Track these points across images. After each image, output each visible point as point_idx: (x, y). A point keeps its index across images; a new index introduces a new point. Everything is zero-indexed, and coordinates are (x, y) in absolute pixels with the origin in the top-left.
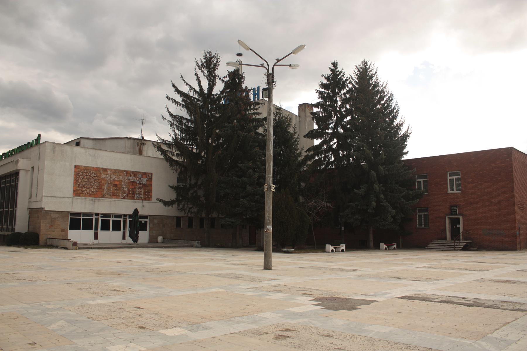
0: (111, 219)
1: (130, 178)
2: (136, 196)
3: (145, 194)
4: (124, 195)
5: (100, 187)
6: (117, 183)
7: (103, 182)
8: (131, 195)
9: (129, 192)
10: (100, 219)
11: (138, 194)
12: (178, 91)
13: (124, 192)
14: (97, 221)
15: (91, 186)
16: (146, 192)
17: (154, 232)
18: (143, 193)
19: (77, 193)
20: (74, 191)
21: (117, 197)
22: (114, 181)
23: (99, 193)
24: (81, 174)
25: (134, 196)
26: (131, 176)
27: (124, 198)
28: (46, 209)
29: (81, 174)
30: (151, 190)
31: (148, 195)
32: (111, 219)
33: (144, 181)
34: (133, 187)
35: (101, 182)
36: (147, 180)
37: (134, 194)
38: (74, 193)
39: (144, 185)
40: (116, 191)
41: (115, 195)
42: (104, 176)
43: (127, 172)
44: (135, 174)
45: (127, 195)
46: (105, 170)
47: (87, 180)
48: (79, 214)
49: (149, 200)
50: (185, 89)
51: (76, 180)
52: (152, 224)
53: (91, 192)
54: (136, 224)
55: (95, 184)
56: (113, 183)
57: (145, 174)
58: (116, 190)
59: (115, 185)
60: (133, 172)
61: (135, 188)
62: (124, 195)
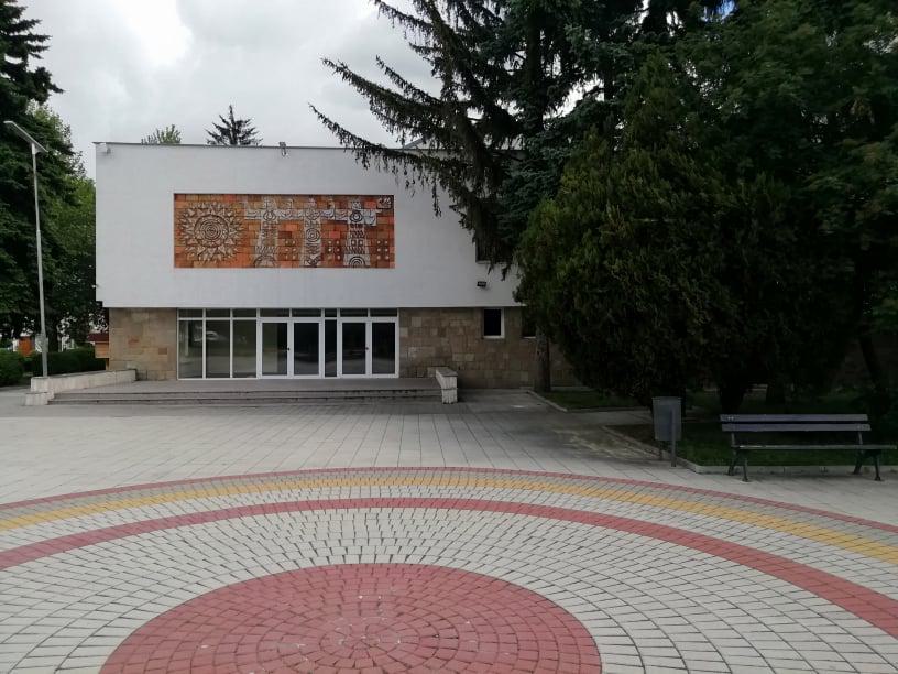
0: (369, 321)
1: (327, 212)
2: (348, 257)
3: (373, 252)
4: (313, 257)
5: (244, 242)
6: (289, 228)
7: (250, 228)
8: (334, 255)
9: (327, 247)
10: (340, 321)
11: (354, 251)
12: (224, 121)
13: (312, 250)
14: (331, 327)
15: (218, 242)
16: (377, 246)
17: (413, 349)
18: (367, 251)
19: (183, 259)
20: (177, 256)
21: (294, 262)
22: (283, 223)
23: (244, 255)
24: (192, 213)
25: (342, 259)
26: (329, 207)
27: (313, 265)
28: (105, 306)
29: (192, 213)
30: (391, 240)
31: (383, 254)
32: (291, 322)
33: (370, 217)
34: (338, 235)
35: (247, 229)
36: (378, 215)
37: (341, 253)
38: (176, 260)
39: (370, 228)
40: (287, 249)
41: (287, 258)
42: (249, 212)
43: (317, 198)
44: (341, 200)
45: (322, 258)
46: (256, 197)
47: (207, 227)
48: (224, 312)
49: (388, 266)
50: (225, 126)
51: (180, 229)
52: (406, 331)
53: (220, 257)
54: (362, 337)
55: (229, 235)
56: (280, 228)
57: (371, 198)
58: (290, 245)
59: (287, 235)
60: (335, 197)
61: (343, 237)
62: (313, 257)
